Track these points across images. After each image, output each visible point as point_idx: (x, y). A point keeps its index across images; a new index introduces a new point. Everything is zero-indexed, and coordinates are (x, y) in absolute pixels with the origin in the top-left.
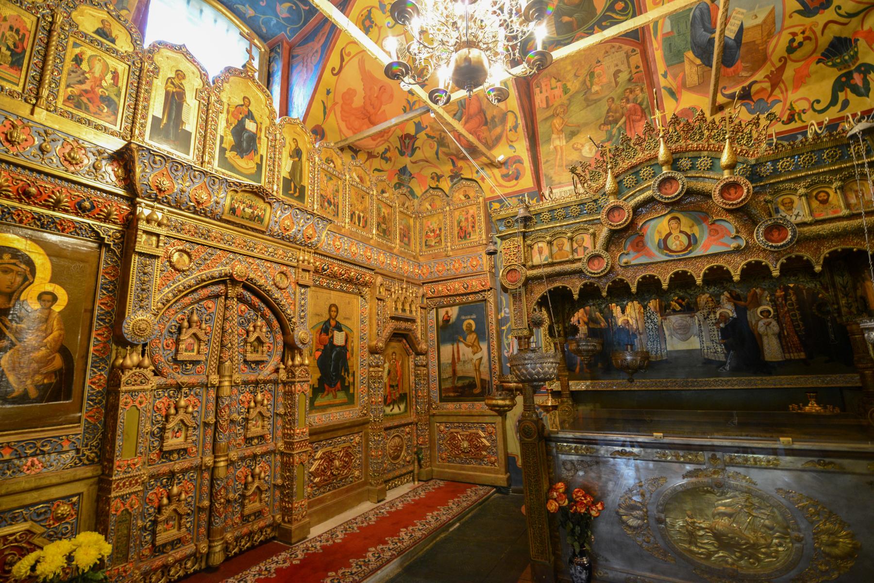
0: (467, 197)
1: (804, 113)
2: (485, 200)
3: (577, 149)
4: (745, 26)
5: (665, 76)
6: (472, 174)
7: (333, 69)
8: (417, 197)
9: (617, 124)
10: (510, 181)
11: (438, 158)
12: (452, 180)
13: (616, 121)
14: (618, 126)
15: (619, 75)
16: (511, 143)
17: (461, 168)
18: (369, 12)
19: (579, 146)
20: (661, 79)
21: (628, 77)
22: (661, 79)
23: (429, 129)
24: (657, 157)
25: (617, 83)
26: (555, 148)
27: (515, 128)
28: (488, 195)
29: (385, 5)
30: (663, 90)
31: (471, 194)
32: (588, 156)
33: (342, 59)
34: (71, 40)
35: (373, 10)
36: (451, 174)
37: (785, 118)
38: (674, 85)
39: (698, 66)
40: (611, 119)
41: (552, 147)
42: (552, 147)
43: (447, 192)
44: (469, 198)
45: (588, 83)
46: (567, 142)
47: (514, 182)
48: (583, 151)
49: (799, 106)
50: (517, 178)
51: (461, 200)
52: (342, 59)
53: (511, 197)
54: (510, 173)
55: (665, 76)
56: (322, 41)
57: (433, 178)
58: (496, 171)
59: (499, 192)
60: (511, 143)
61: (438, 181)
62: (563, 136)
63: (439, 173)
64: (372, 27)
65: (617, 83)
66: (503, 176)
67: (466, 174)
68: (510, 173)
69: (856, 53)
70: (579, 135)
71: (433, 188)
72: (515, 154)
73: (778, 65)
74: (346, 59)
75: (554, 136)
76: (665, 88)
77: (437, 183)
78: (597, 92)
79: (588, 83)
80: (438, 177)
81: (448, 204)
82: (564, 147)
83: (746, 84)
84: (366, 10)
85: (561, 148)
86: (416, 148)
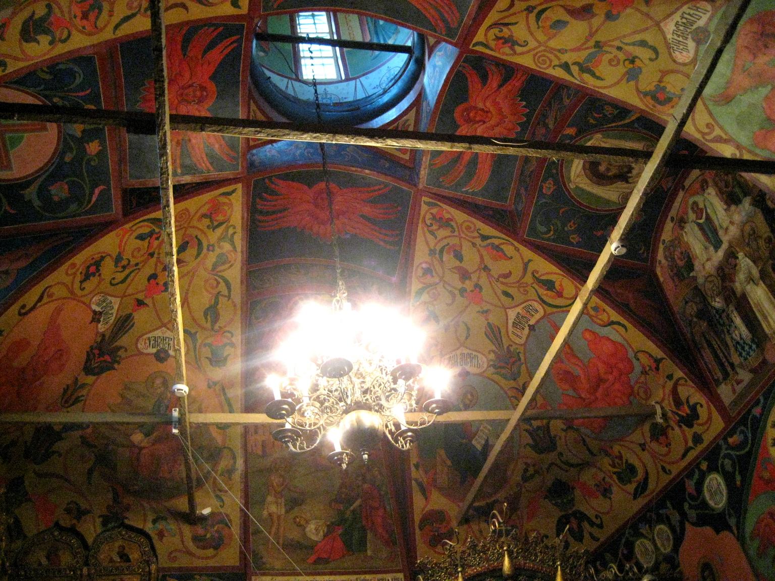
0: (124, 557)
2: (158, 570)
3: (299, 525)
5: (417, 466)
6: (145, 521)
7: (24, 307)
8: (25, 536)
10: (204, 548)
11: (89, 478)
12: (104, 524)
14: (352, 508)
16: (219, 493)
17: (128, 508)
18: (102, 258)
19: (303, 522)
20: (413, 469)
22: (413, 469)
23: (89, 431)
24: (501, 569)
26: (270, 515)
28: (164, 562)
29: (122, 259)
30: (413, 482)
31: (135, 556)
32: (314, 538)
33: (41, 299)
35: (108, 259)
36: (105, 512)
38: (424, 480)
39: (449, 466)
41: (265, 513)
42: (265, 513)
43: (90, 541)
44: (128, 560)
46: (287, 512)
47: (210, 552)
48: (307, 529)
50: (216, 548)
51: (111, 560)
52: (41, 299)
53: (201, 575)
54: (208, 536)
55: (417, 466)
56: (22, 264)
57: (68, 511)
58: (187, 530)
59: (184, 562)
60: (219, 493)
61: (79, 519)
63: (84, 505)
64: (94, 274)
66: (196, 539)
67: (134, 521)
68: (208, 536)
69: (573, 499)
70: (303, 507)
71: (62, 529)
74: (45, 299)
75: (270, 499)
76: (416, 480)
77: (74, 521)
80: (81, 513)
81: (86, 564)
82: (283, 517)
84: (99, 255)
85: (279, 517)
86: (54, 452)
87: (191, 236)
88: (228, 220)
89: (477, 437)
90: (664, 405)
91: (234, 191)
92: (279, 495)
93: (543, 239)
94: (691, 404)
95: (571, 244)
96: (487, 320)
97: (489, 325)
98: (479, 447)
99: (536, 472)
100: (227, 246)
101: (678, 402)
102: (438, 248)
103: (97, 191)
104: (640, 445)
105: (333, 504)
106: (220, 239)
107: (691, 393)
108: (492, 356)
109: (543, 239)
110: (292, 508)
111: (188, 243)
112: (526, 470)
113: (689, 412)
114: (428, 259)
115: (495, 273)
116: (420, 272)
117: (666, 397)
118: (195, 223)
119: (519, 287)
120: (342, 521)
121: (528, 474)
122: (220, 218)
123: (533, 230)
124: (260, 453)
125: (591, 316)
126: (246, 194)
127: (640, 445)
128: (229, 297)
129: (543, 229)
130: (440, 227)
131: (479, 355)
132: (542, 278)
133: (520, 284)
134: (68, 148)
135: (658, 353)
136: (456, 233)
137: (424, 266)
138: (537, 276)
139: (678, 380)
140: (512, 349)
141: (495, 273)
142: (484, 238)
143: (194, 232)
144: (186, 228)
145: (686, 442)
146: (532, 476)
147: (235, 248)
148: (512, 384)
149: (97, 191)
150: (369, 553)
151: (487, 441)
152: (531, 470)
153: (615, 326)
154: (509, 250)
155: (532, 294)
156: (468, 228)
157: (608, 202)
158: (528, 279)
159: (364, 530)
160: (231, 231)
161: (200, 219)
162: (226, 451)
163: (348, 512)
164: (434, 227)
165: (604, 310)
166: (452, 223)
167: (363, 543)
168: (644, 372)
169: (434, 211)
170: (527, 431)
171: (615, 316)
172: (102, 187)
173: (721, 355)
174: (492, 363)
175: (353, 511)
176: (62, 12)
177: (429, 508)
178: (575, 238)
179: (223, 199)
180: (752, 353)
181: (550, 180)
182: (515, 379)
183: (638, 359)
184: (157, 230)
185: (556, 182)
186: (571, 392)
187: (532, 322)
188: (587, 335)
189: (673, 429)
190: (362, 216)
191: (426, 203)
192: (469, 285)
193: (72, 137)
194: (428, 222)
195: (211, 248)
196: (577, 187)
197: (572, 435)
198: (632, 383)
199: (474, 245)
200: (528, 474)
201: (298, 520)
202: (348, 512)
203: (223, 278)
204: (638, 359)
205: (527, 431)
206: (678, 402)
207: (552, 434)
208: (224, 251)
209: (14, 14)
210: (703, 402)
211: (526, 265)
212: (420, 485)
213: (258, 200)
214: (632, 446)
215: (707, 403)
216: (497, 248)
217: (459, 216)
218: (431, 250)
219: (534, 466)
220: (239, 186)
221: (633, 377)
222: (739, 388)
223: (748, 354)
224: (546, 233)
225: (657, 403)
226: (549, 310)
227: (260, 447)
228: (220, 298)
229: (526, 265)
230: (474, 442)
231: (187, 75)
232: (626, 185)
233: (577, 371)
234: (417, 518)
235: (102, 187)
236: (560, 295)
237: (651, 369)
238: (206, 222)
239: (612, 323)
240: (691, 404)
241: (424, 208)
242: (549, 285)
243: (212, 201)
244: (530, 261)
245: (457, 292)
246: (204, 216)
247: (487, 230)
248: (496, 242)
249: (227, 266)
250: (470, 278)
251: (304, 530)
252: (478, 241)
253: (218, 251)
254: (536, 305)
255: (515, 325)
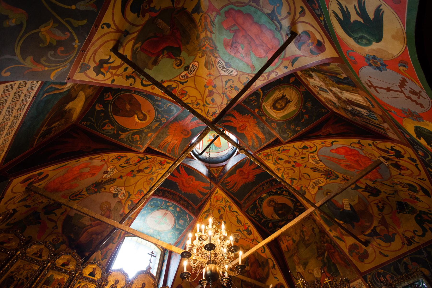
1: (414, 238)
4: (353, 204)
5: (330, 231)
9: (324, 255)
13: (323, 254)
15: (314, 230)
19: (311, 271)
20: (330, 232)
21: (319, 231)
22: (330, 232)
25: (315, 234)
27: (274, 266)
34: (79, 281)
37: (406, 242)
40: (320, 253)
45: (302, 236)
46: (304, 269)
48: (314, 274)
49: (409, 235)
55: (330, 231)
62: (301, 266)
65: (315, 234)
72: (279, 282)
73: (380, 217)
75: (297, 267)
76: (334, 236)
78: (308, 240)
79: (302, 236)
83: (372, 228)
87: (218, 208)
88: (223, 198)
89: (345, 206)
90: (383, 155)
91: (218, 190)
92: (299, 263)
93: (290, 137)
94: (390, 148)
95: (299, 131)
96: (309, 168)
97: (311, 168)
98: (349, 209)
99: (383, 204)
100: (228, 203)
101: (386, 151)
102: (274, 162)
103: (187, 216)
104: (399, 174)
105: (318, 258)
106: (226, 203)
107: (382, 145)
108: (323, 176)
109: (290, 137)
110: (305, 267)
111: (219, 210)
112: (378, 207)
113: (394, 152)
114: (275, 166)
115: (293, 155)
116: (277, 171)
117: (379, 152)
118: (216, 204)
119: (302, 154)
120: (325, 265)
121: (381, 207)
122: (221, 199)
123: (285, 139)
124: (287, 250)
125: (325, 146)
126: (222, 189)
127: (399, 174)
128: (239, 215)
129: (286, 136)
130: (268, 157)
131: (319, 179)
132: (302, 147)
133: (302, 153)
134: (174, 213)
135: (355, 140)
136: (273, 155)
137: (276, 169)
138: (300, 148)
139: (373, 143)
140: (325, 170)
141: (293, 155)
142: (279, 150)
143: (218, 206)
144: (215, 207)
145: (413, 164)
146: (383, 207)
147: (229, 202)
148: (339, 180)
149: (187, 216)
150: (342, 274)
151: (350, 205)
152: (380, 205)
153: (334, 143)
154: (285, 148)
155: (308, 153)
156: (273, 151)
157: (294, 111)
158: (300, 150)
159: (334, 265)
160: (226, 199)
161: (216, 202)
162: (269, 259)
163: (325, 259)
164: (267, 158)
165: (325, 142)
166: (269, 154)
167: (337, 270)
168: (362, 150)
169: (262, 155)
170: (363, 191)
171: (331, 141)
172: (187, 215)
173: (372, 124)
174: (326, 178)
175: (327, 258)
176: (135, 199)
177: (348, 245)
178: (298, 129)
179: (217, 195)
180: (375, 116)
181: (272, 124)
182: (338, 178)
183: (354, 147)
184: (208, 213)
185: (274, 122)
186: (356, 170)
187: (318, 160)
188: (334, 151)
189: (399, 162)
190: (253, 169)
191: (259, 155)
192: (293, 163)
193: (172, 211)
194: (265, 158)
195: (225, 206)
196: (280, 117)
197: (378, 184)
198: (365, 155)
199: (279, 154)
200: (381, 207)
201: (309, 271)
202: (325, 259)
203: (234, 211)
204: (354, 147)
205: (363, 191)
206: (386, 151)
207: (373, 187)
208: (229, 205)
209: (124, 209)
210: (392, 145)
211: (294, 147)
212: (337, 237)
213: (226, 187)
214: (396, 177)
215: (395, 144)
216: (284, 150)
217: (268, 151)
218: (273, 164)
219: (380, 202)
220: (218, 189)
221: (361, 152)
222: (391, 131)
223: (375, 117)
224: (288, 135)
225: (379, 157)
226: (316, 152)
227: (286, 248)
228: (237, 216)
229: (294, 147)
230: (345, 209)
231: (184, 179)
232: (292, 103)
233: (348, 163)
234: (346, 251)
235: (187, 215)
236: (311, 147)
237: (362, 147)
238: (218, 202)
239: (332, 143)
240: (390, 148)
241: (259, 156)
242: (305, 147)
243: (214, 198)
244: (293, 146)
245: (292, 168)
246: (216, 202)
247: (277, 148)
248: (282, 149)
249: (232, 208)
250: (291, 162)
251: (313, 275)
252: (279, 152)
253: (227, 206)
254: (313, 155)
255: (316, 163)
